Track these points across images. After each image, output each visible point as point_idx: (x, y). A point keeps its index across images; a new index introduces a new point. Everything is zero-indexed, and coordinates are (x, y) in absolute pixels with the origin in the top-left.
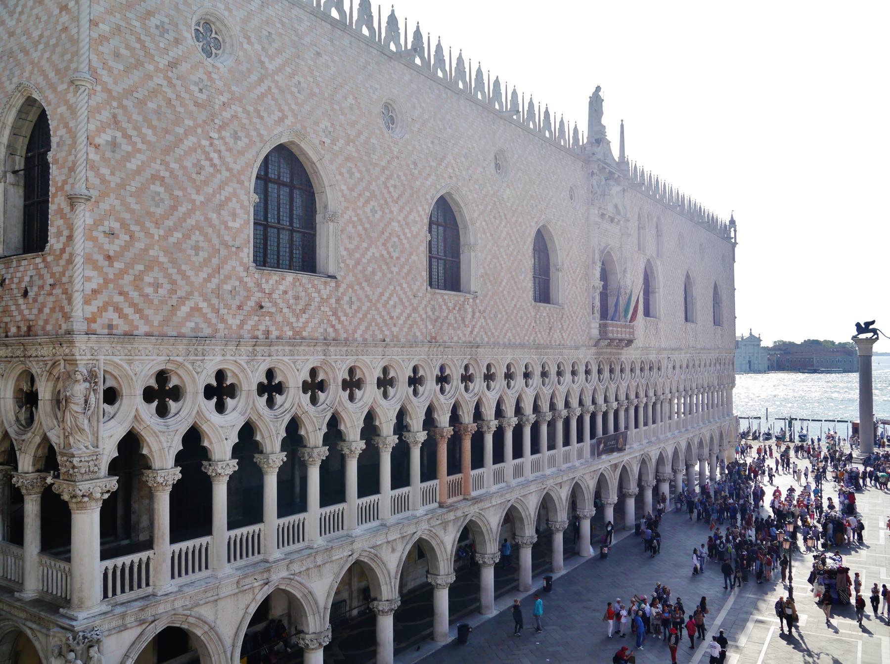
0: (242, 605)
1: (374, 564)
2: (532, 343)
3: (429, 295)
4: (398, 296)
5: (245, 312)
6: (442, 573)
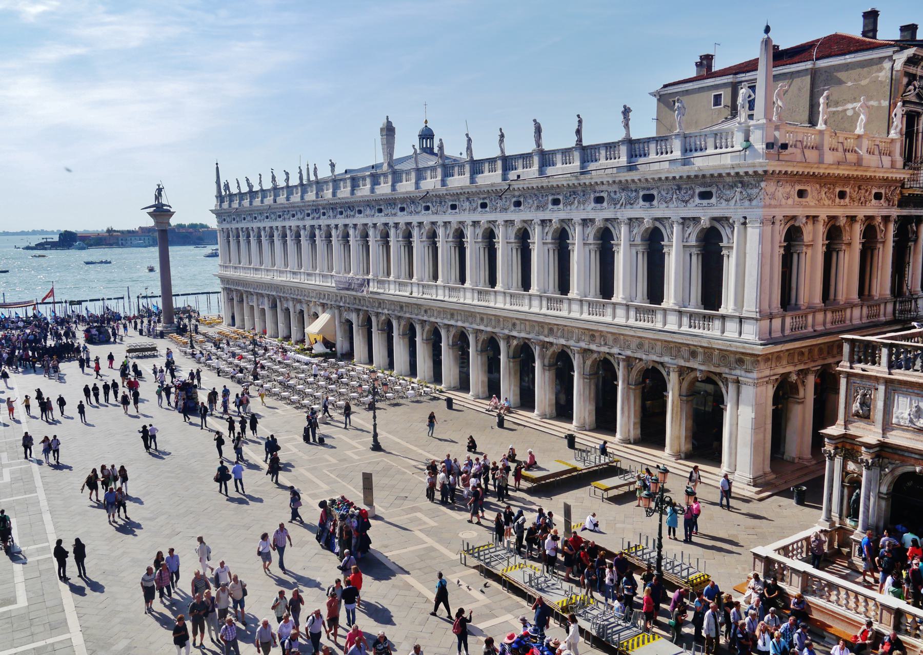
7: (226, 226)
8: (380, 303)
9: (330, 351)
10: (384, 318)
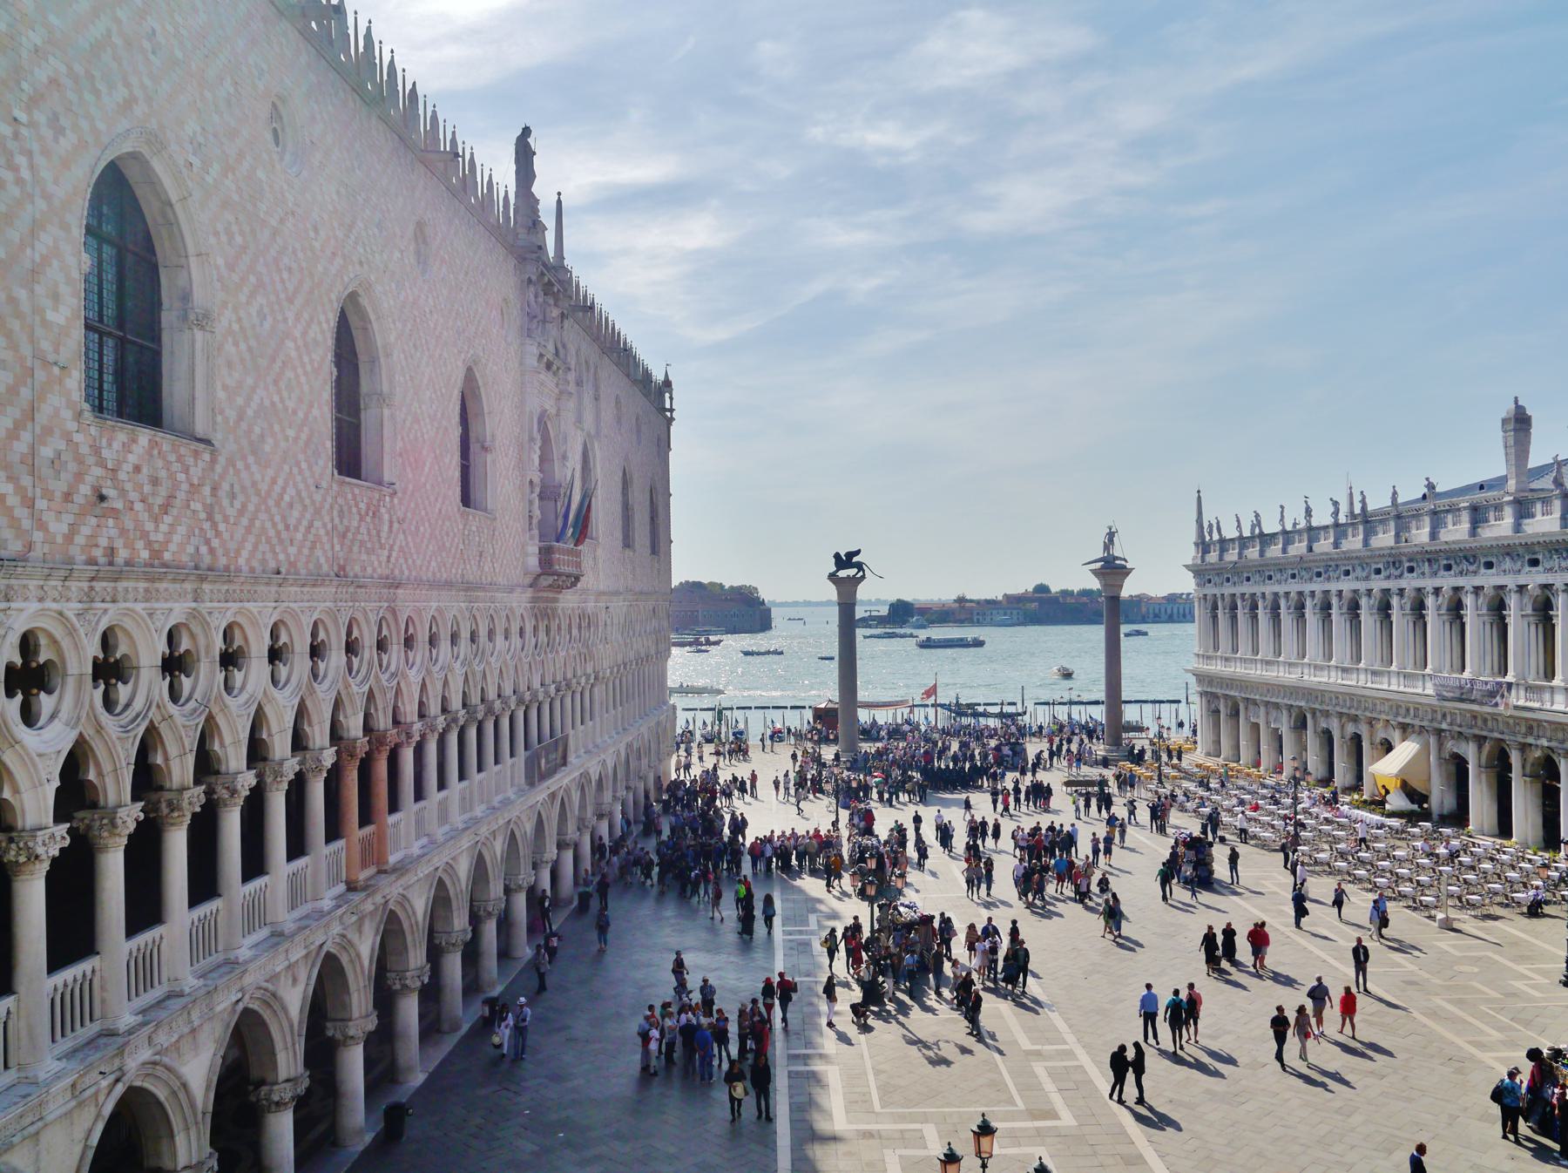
0: (79, 1134)
1: (268, 1012)
2: (460, 580)
3: (335, 486)
4: (295, 485)
5: (75, 508)
6: (356, 1014)
7: (1210, 590)
8: (1531, 728)
9: (1418, 807)
10: (1538, 754)
